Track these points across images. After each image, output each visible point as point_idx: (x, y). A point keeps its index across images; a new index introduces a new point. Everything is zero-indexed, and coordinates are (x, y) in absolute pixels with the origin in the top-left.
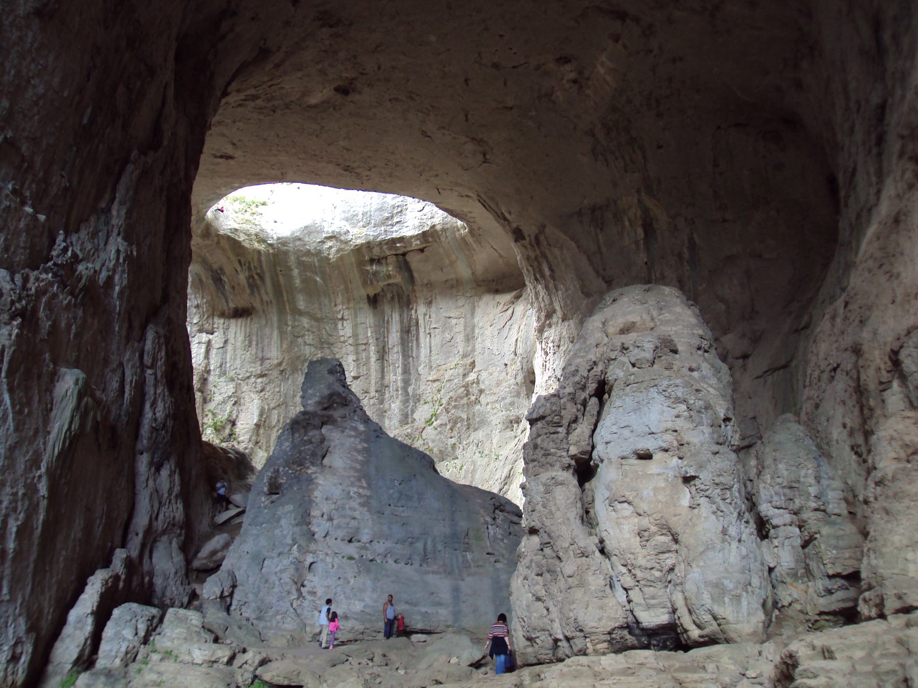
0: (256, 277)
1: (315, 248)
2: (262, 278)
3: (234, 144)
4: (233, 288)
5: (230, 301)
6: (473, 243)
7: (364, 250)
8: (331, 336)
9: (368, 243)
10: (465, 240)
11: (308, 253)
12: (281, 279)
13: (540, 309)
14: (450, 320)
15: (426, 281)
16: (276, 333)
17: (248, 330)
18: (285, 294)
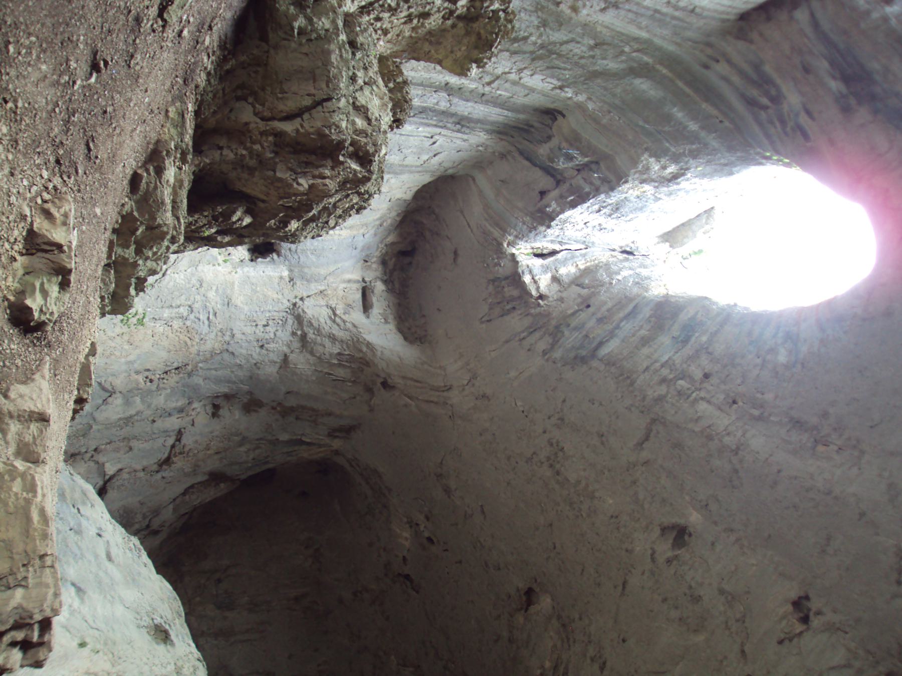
0: (765, 101)
1: (687, 163)
2: (751, 103)
3: (624, 584)
4: (807, 70)
5: (809, 30)
6: (492, 230)
7: (612, 177)
8: (548, 68)
9: (612, 189)
10: (501, 229)
11: (694, 155)
12: (715, 112)
13: (318, 331)
14: (432, 154)
15: (509, 157)
16: (644, 35)
17: (705, 13)
18: (688, 90)
